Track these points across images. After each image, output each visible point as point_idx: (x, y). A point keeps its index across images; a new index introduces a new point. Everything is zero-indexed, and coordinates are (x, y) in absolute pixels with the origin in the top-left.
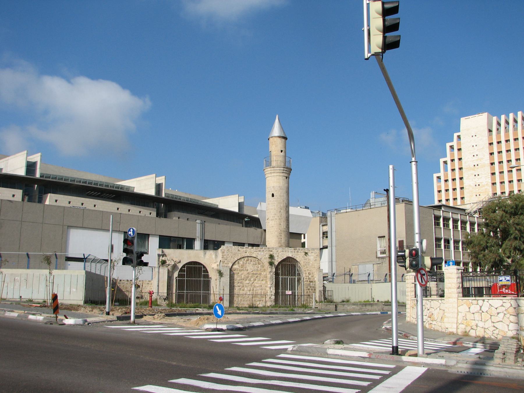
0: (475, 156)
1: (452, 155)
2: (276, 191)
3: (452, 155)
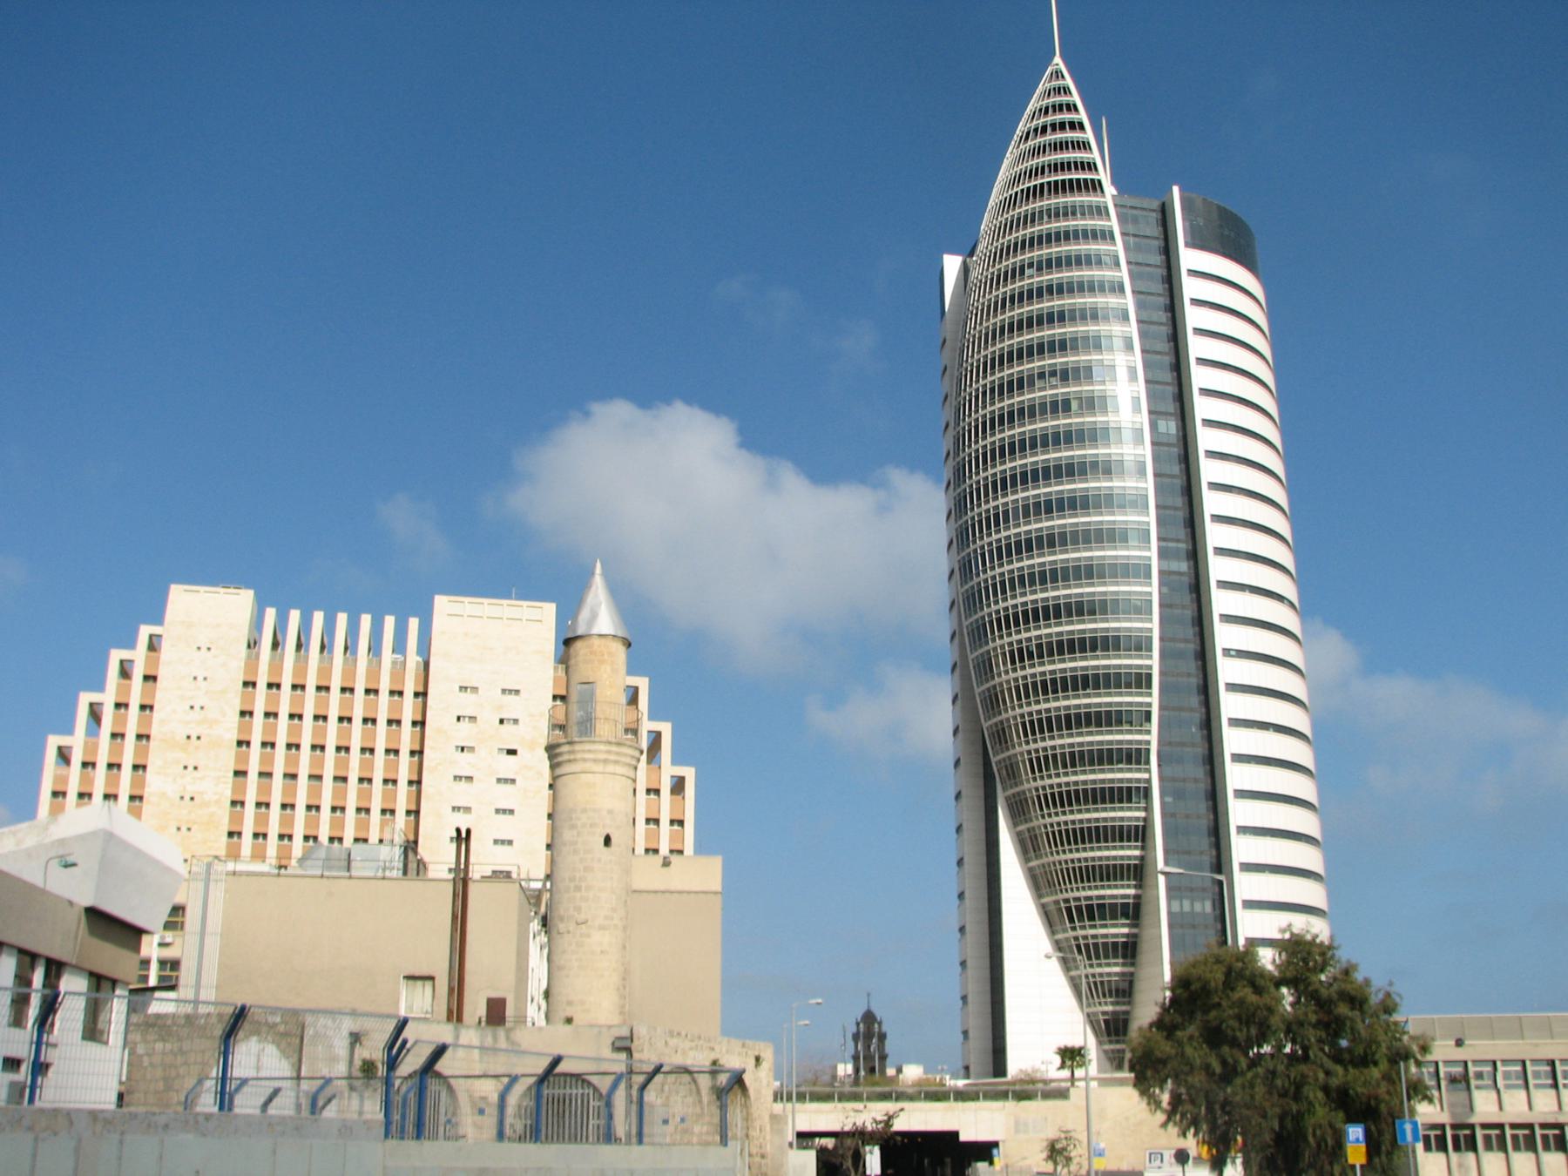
0: (197, 708)
1: (124, 690)
3: (124, 690)
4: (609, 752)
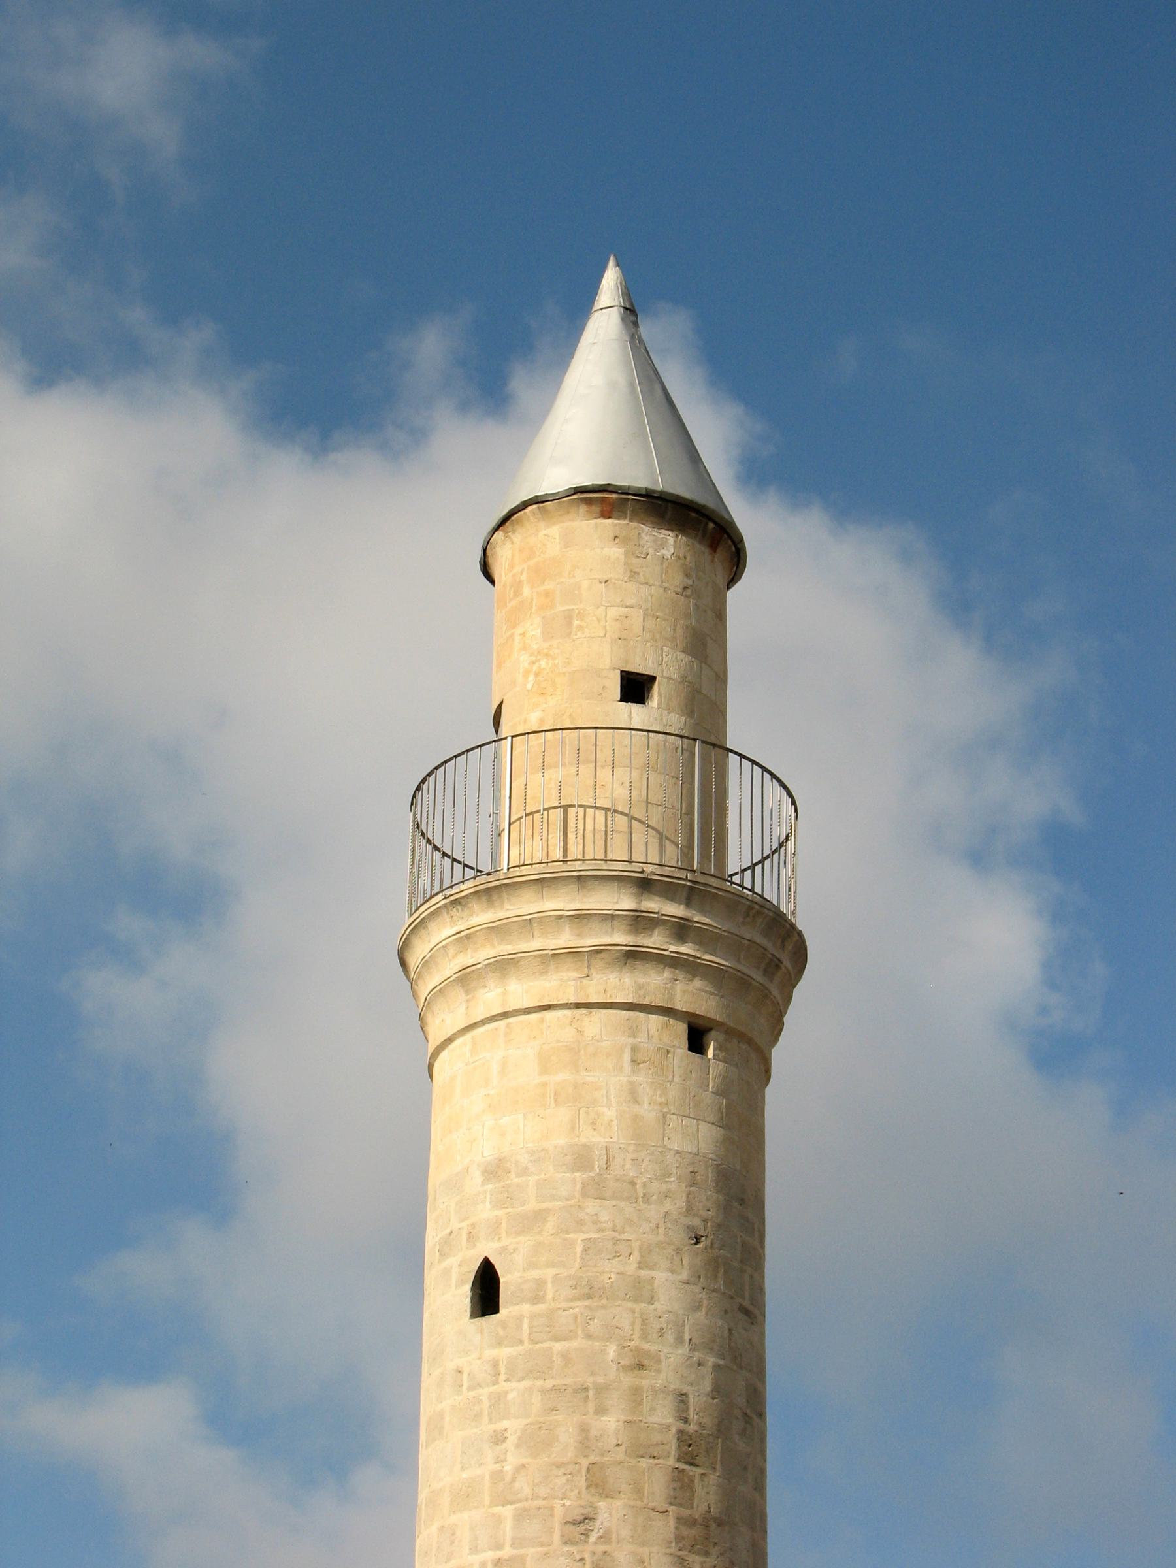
2: (532, 1221)
4: (465, 939)
